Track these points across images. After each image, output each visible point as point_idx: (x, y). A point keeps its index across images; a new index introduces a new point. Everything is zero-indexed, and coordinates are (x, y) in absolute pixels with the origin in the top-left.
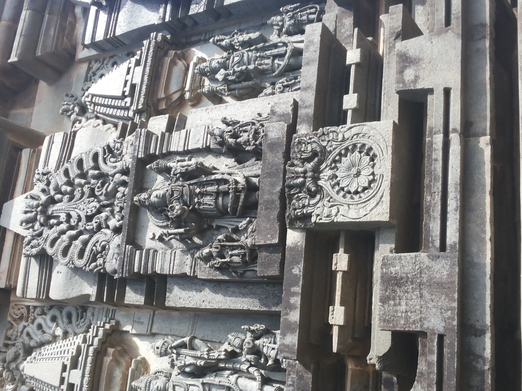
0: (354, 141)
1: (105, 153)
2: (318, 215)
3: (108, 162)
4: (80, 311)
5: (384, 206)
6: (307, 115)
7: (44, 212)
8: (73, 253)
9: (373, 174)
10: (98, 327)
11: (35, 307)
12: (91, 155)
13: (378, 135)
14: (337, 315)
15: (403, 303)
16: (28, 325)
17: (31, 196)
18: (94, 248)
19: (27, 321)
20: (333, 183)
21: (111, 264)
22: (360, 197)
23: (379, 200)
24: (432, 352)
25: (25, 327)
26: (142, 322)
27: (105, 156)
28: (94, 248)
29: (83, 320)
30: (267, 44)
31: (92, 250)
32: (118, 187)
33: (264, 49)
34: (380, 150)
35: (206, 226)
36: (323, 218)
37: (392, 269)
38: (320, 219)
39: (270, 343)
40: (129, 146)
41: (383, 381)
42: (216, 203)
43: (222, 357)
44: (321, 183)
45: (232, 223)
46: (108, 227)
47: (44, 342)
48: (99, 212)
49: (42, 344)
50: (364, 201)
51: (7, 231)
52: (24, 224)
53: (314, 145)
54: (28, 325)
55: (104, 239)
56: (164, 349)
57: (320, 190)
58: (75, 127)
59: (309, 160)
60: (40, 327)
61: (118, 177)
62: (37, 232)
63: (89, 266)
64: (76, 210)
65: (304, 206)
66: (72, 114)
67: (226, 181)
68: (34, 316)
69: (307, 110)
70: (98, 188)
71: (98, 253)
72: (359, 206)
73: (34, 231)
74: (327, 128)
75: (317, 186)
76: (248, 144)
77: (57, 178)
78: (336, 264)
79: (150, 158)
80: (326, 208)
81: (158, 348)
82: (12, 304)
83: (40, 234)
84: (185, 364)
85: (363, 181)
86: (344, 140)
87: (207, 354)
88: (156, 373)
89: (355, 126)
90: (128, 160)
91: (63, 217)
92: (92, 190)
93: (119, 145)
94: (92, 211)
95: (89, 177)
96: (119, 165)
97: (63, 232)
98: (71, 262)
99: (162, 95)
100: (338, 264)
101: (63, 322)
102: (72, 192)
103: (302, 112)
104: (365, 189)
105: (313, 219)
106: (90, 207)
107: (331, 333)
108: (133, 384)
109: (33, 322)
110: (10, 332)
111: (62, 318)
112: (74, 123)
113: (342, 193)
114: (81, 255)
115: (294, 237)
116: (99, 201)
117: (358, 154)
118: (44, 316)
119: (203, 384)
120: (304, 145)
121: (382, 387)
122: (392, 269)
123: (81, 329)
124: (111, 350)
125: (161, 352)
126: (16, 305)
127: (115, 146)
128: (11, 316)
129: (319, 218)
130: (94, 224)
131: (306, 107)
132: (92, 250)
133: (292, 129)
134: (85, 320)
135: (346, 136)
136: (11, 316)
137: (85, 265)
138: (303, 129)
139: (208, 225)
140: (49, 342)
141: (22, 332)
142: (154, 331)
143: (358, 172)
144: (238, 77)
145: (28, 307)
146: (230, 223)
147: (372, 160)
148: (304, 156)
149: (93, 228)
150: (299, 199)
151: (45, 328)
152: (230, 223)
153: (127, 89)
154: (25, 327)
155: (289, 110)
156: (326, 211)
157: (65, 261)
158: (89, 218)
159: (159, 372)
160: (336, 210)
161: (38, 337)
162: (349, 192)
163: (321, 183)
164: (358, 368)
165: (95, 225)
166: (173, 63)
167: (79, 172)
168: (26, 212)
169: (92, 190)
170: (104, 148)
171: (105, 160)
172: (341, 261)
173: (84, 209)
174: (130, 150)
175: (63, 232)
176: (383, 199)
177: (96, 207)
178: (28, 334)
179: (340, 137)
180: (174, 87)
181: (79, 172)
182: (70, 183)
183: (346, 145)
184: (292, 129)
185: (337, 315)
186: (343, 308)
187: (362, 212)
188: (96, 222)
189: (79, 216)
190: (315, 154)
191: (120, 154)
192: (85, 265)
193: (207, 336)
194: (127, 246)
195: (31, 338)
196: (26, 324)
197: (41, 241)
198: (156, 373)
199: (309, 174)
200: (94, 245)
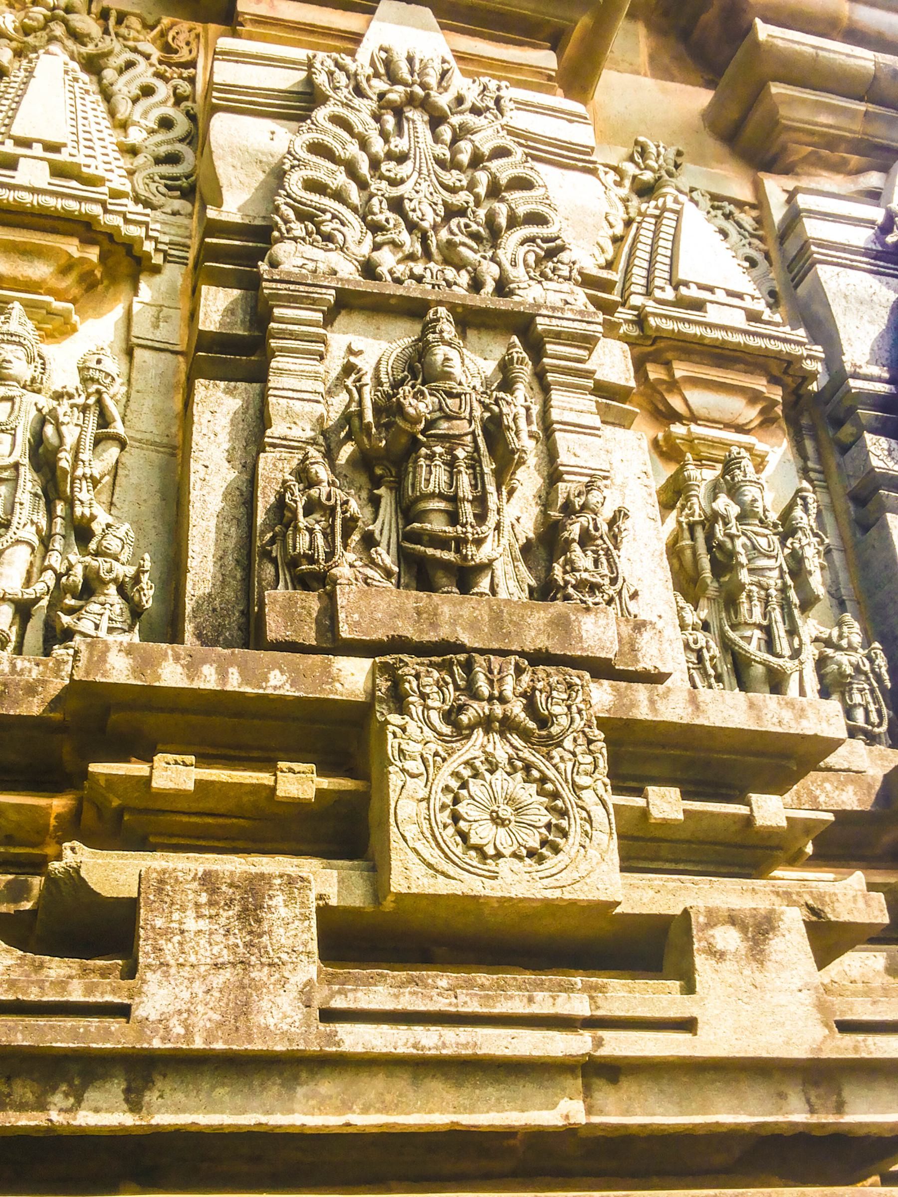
0: (575, 812)
1: (546, 240)
2: (404, 730)
3: (526, 248)
4: (184, 183)
5: (425, 880)
6: (633, 705)
7: (411, 100)
8: (317, 167)
9: (499, 855)
10: (147, 224)
11: (192, 80)
12: (541, 209)
13: (589, 867)
14: (174, 774)
15: (203, 924)
16: (152, 65)
17: (448, 70)
18: (328, 216)
19: (161, 62)
20: (477, 763)
21: (291, 256)
22: (445, 826)
23: (440, 868)
24: (90, 989)
25: (147, 57)
26: (158, 327)
27: (539, 241)
28: (328, 216)
29: (163, 190)
30: (796, 612)
31: (324, 211)
32: (468, 272)
33: (786, 605)
34: (555, 871)
35: (379, 471)
36: (397, 740)
37: (279, 900)
38: (395, 736)
39: (110, 619)
40: (564, 296)
41: (22, 878)
42: (432, 496)
43: (78, 510)
44: (479, 733)
45: (386, 532)
46: (377, 247)
47: (113, 100)
48: (412, 226)
49: (107, 95)
50: (437, 834)
51: (367, 16)
52: (383, 55)
53: (564, 721)
54: (152, 65)
55: (349, 238)
56: (97, 375)
57: (462, 732)
58: (606, 173)
59: (531, 708)
60: (148, 91)
61: (489, 272)
62: (364, 85)
63: (286, 204)
64: (416, 174)
65: (424, 696)
66: (637, 165)
67: (481, 518)
68: (172, 78)
69: (643, 704)
70: (467, 226)
71: (317, 225)
72: (425, 825)
73: (368, 79)
74: (604, 751)
75: (472, 727)
76: (568, 568)
77: (490, 132)
78: (291, 770)
79: (535, 347)
80: (419, 747)
81: (99, 362)
82: (199, 27)
83: (359, 92)
84: (63, 424)
85: (483, 833)
86: (576, 788)
87: (84, 475)
88: (41, 358)
89: (608, 815)
90: (528, 293)
91: (400, 144)
92: (462, 212)
93: (566, 273)
94: (414, 210)
95: (492, 206)
96: (518, 274)
97: (364, 145)
98: (296, 162)
99: (681, 370)
100: (291, 775)
101: (158, 145)
102: (458, 166)
103: (641, 691)
104: (464, 836)
105: (395, 719)
106: (422, 207)
107: (134, 759)
108: (16, 305)
109: (158, 75)
110: (134, 22)
111: (168, 142)
112: (616, 169)
113: (454, 784)
114: (313, 186)
115: (352, 677)
116: (435, 227)
117: (545, 820)
118: (172, 100)
119: (16, 466)
120: (565, 696)
121: (10, 877)
122: (279, 900)
123: (142, 186)
124: (93, 254)
125: (89, 368)
126: (198, 36)
127: (562, 263)
128: (173, 25)
129: (398, 731)
130: (384, 215)
131: (652, 702)
132: (324, 211)
133: (601, 669)
134: (164, 195)
135: (585, 794)
136: (173, 25)
137: (289, 196)
138: (601, 695)
139: (382, 477)
140: (112, 113)
141: (135, 50)
142: (138, 352)
143: (503, 820)
144: (721, 546)
145: (192, 64)
146: (386, 527)
147: (531, 854)
148: (541, 698)
149: (374, 214)
150: (441, 686)
151: (145, 103)
152: (386, 527)
153: (693, 292)
154: (147, 57)
155: (645, 664)
156: (413, 748)
157: (298, 150)
158: (397, 205)
159: (43, 364)
160: (416, 772)
161: (124, 87)
162: (456, 801)
163: (479, 733)
164: (53, 822)
165: (381, 218)
166: (754, 397)
167: (503, 181)
168: (410, 60)
169: (462, 212)
170: (558, 238)
171: (531, 240)
172: (298, 782)
173: (417, 192)
174: (555, 299)
175: (364, 145)
176: (441, 878)
177: (422, 220)
178: (130, 65)
179: (582, 780)
180: (698, 399)
181: (503, 181)
182: (477, 161)
183: (566, 793)
184: (601, 669)
185: (174, 774)
186: (190, 786)
187: (411, 831)
188: (387, 220)
189: (402, 181)
190: (544, 722)
191: (543, 274)
192: (289, 196)
193: (127, 476)
194: (333, 292)
195: (121, 72)
196: (154, 60)
197: (345, 93)
198: (41, 358)
199: (498, 710)
200: (334, 217)
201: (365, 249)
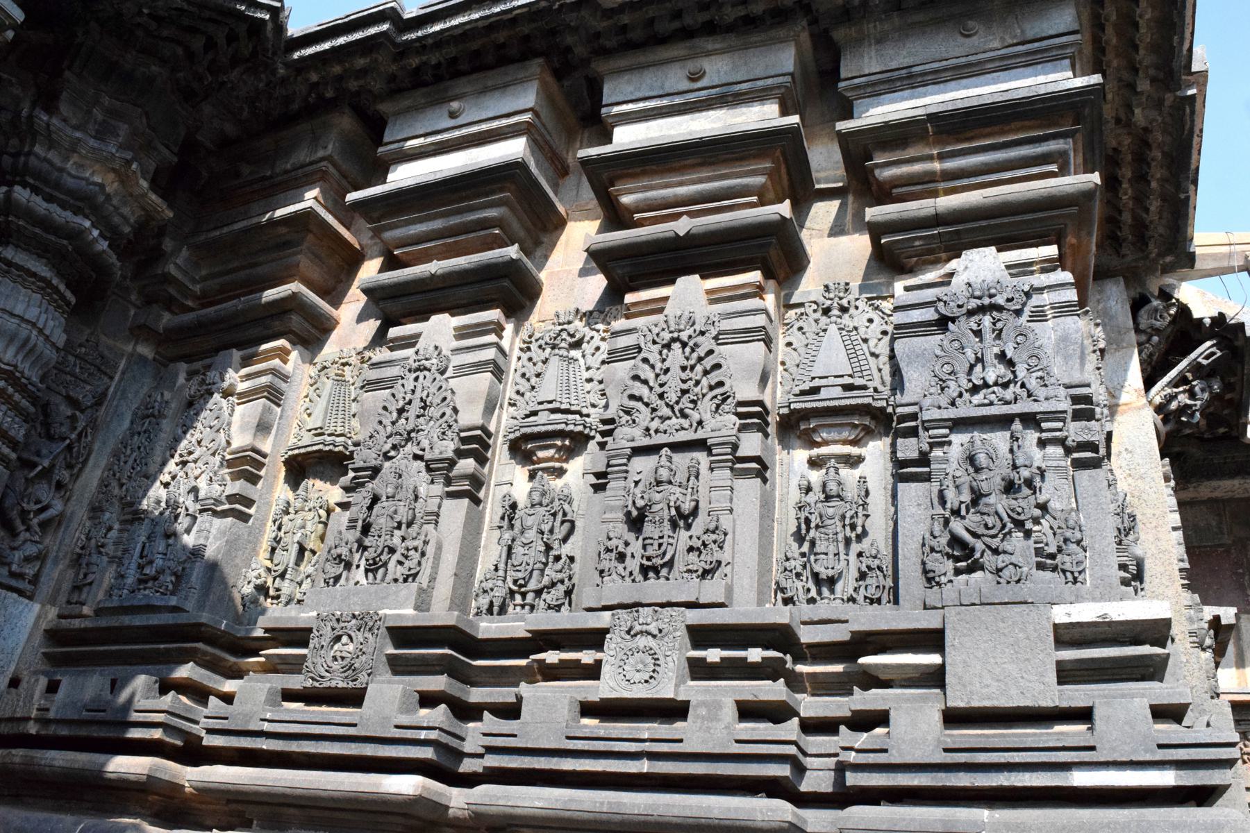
25: (598, 331)
46: (653, 419)
48: (667, 405)
79: (709, 450)
97: (653, 367)
114: (632, 397)
116: (677, 402)
130: (657, 403)
154: (598, 331)
158: (661, 396)
178: (592, 338)
201: (646, 424)
